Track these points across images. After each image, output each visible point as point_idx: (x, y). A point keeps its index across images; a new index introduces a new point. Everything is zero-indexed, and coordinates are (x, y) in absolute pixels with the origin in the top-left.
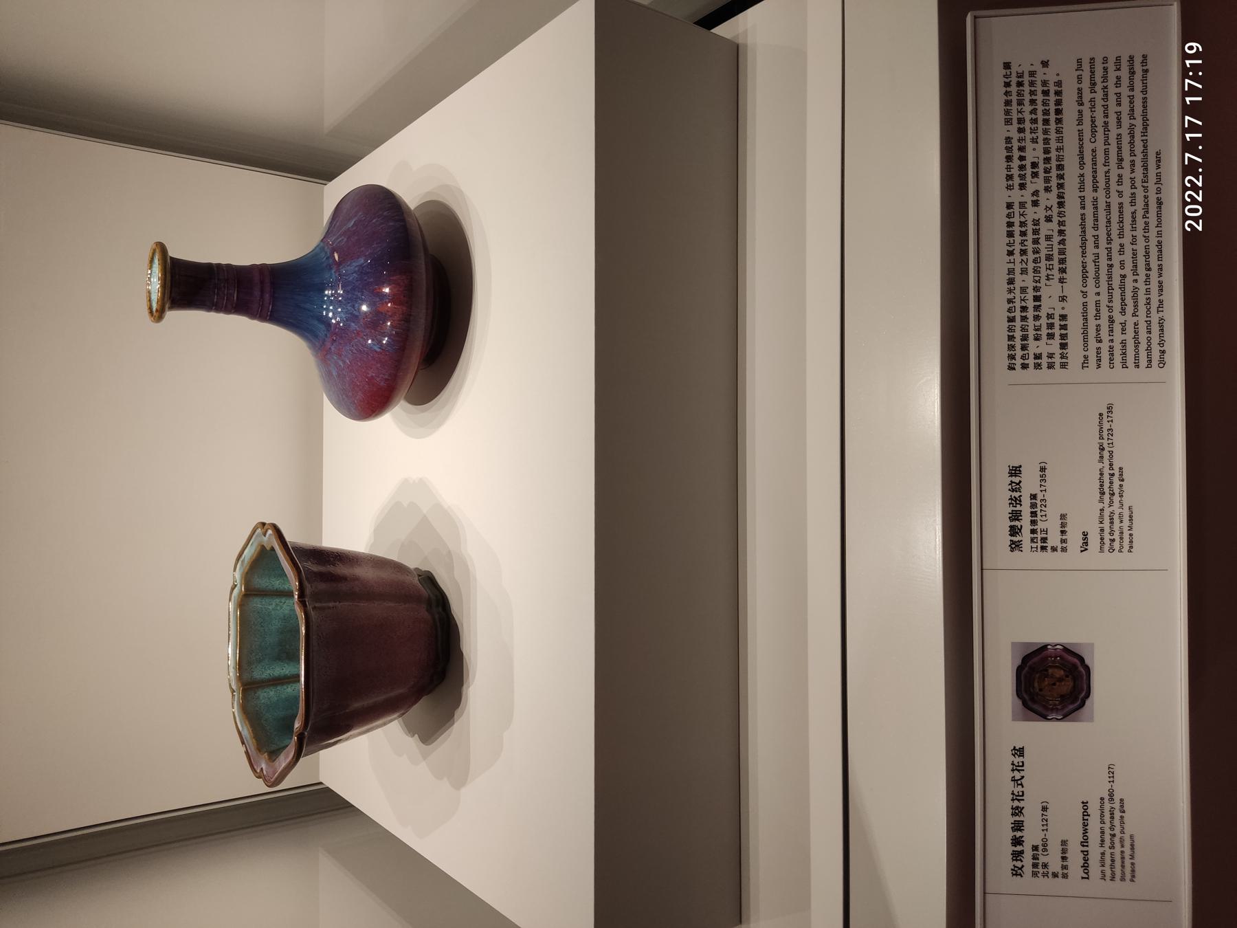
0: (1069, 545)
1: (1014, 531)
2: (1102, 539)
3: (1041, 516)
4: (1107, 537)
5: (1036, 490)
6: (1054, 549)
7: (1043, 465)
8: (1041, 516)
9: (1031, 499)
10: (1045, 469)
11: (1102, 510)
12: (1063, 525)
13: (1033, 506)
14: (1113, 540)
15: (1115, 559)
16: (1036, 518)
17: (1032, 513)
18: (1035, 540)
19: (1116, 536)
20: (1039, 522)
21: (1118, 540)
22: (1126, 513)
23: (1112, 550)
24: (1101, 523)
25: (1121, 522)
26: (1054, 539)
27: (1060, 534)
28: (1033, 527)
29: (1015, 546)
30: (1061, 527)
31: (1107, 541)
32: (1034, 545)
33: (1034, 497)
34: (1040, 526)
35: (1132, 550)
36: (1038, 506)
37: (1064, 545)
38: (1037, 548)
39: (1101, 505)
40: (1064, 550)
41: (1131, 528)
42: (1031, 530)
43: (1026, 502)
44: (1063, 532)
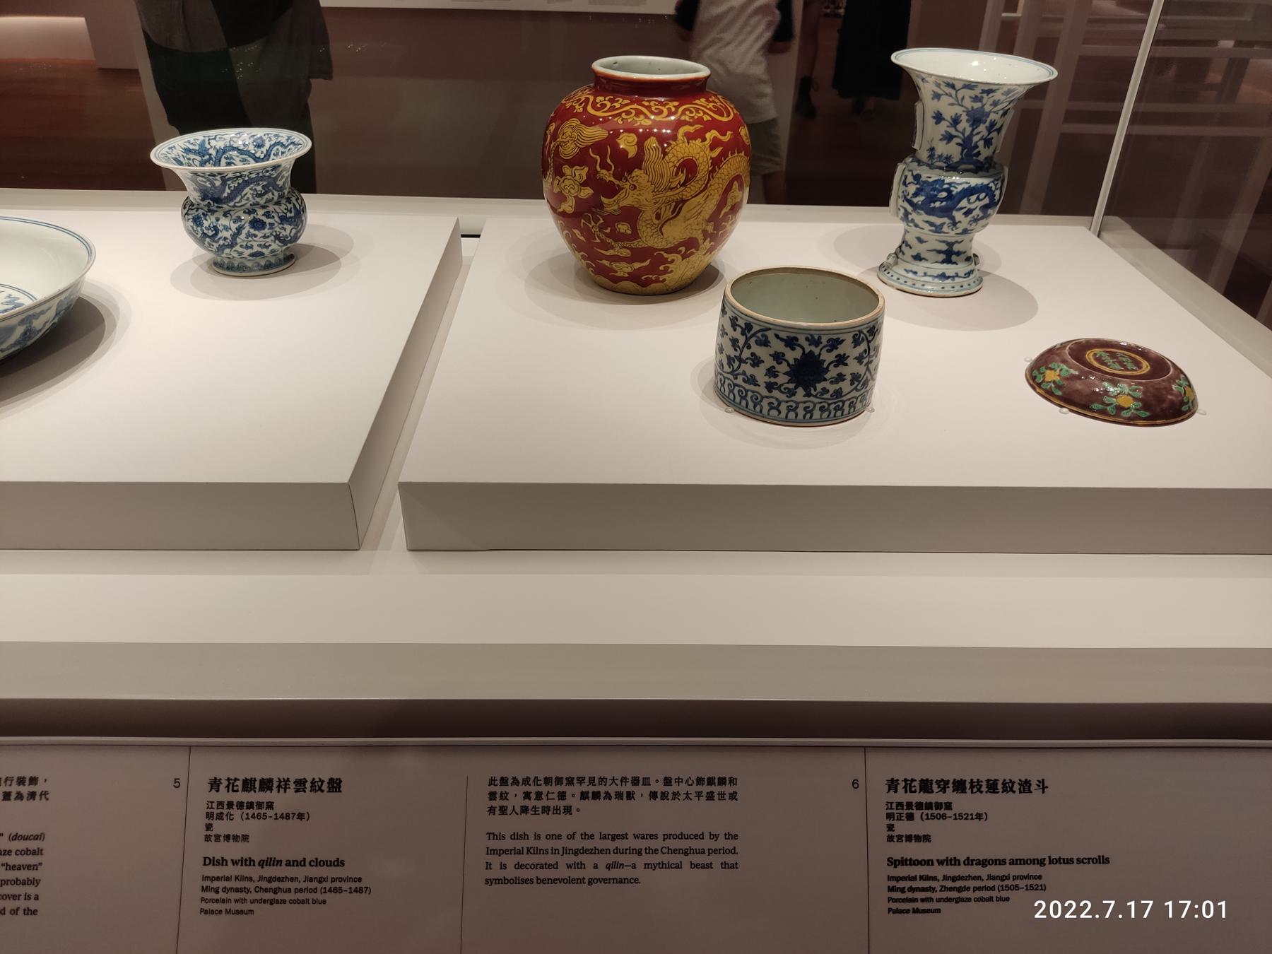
0: (213, 844)
1: (231, 785)
3: (247, 814)
6: (209, 827)
9: (267, 803)
12: (236, 838)
13: (260, 805)
17: (252, 803)
18: (220, 807)
26: (220, 827)
27: (226, 834)
29: (215, 784)
30: (233, 836)
32: (215, 805)
33: (270, 805)
34: (236, 812)
36: (260, 811)
37: (213, 839)
38: (212, 808)
43: (264, 797)
44: (227, 837)
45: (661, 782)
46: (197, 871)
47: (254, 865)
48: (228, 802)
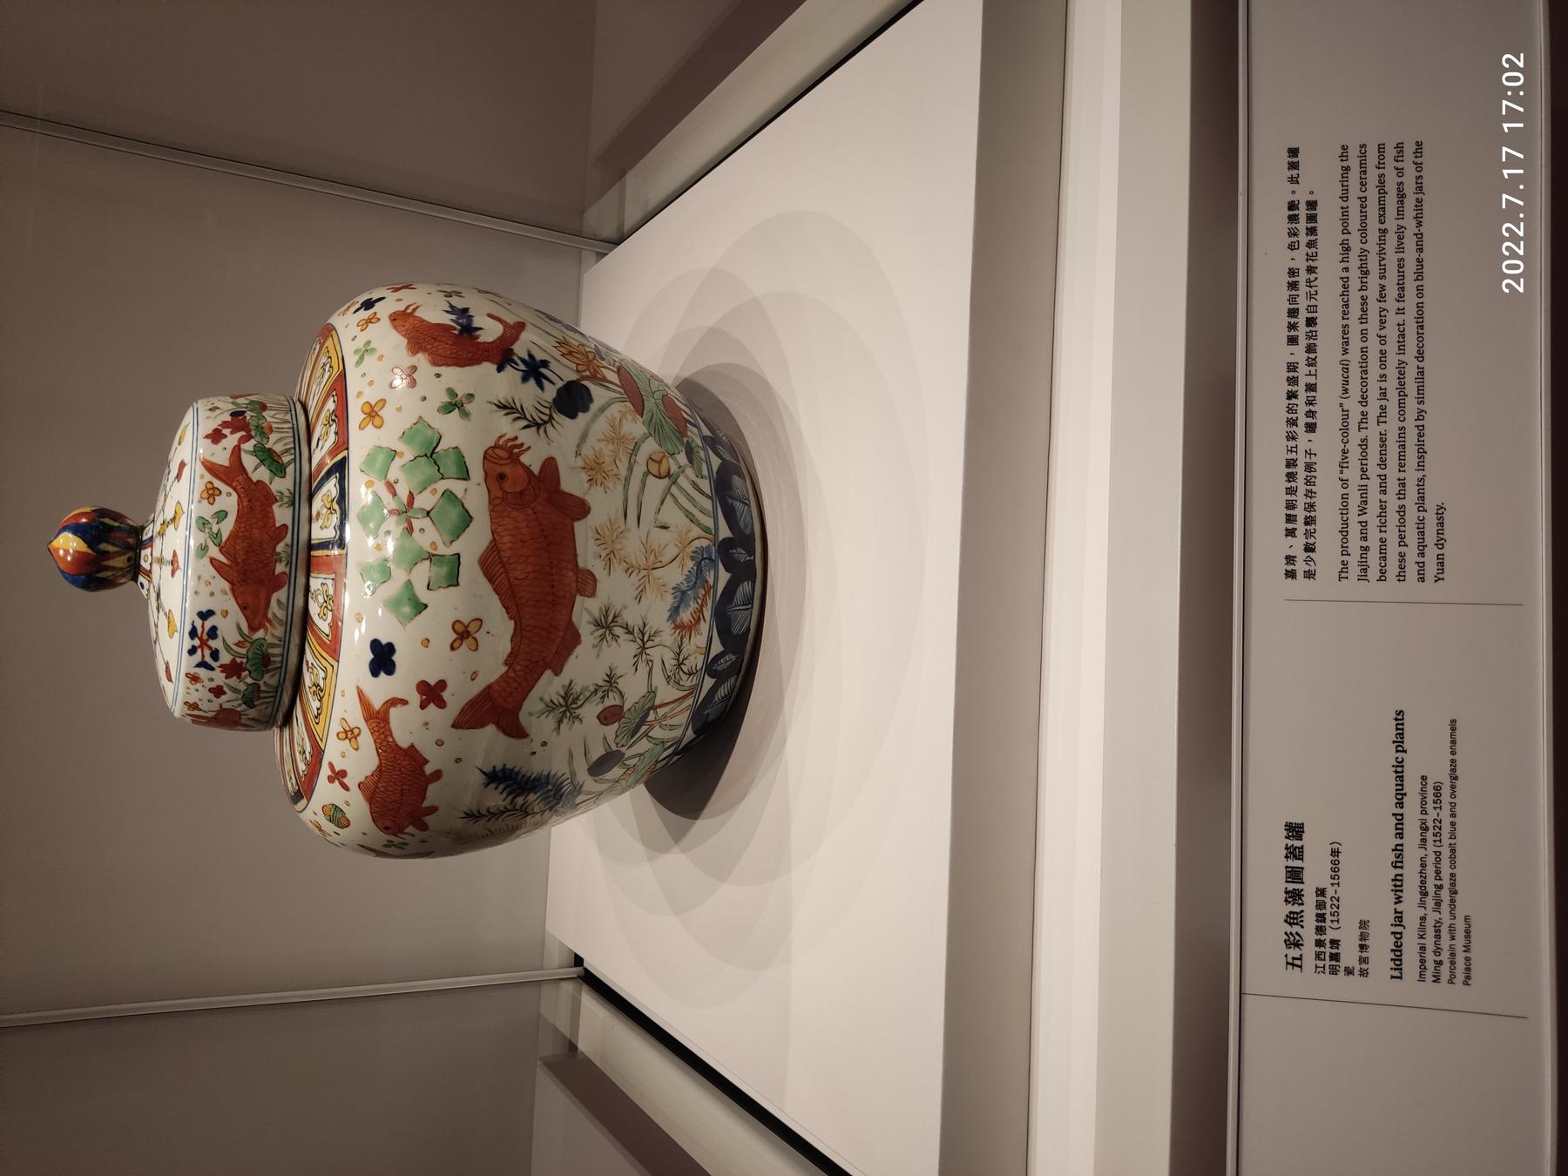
0: (1371, 967)
1: (1294, 942)
2: (1423, 961)
3: (1332, 921)
4: (1430, 958)
5: (1325, 882)
6: (1349, 971)
7: (1335, 846)
8: (1332, 921)
10: (1338, 852)
11: (1423, 919)
12: (1363, 937)
13: (1321, 905)
14: (1440, 963)
15: (1442, 993)
16: (1323, 924)
17: (1318, 915)
18: (1322, 957)
19: (1445, 956)
20: (1329, 931)
21: (1447, 964)
22: (1460, 926)
23: (1437, 980)
24: (1421, 937)
25: (1453, 938)
26: (1349, 956)
27: (1358, 949)
28: (1318, 937)
29: (1295, 963)
31: (1430, 965)
32: (1320, 963)
33: (1321, 892)
34: (1330, 935)
35: (1469, 982)
36: (1328, 906)
37: (1364, 966)
38: (1324, 967)
39: (1421, 912)
40: (1364, 973)
41: (1467, 949)
42: (1316, 940)
43: (1310, 899)
44: (1363, 947)
45: (1293, 348)
46: (1410, 987)
47: (1402, 845)
48: (1316, 946)
